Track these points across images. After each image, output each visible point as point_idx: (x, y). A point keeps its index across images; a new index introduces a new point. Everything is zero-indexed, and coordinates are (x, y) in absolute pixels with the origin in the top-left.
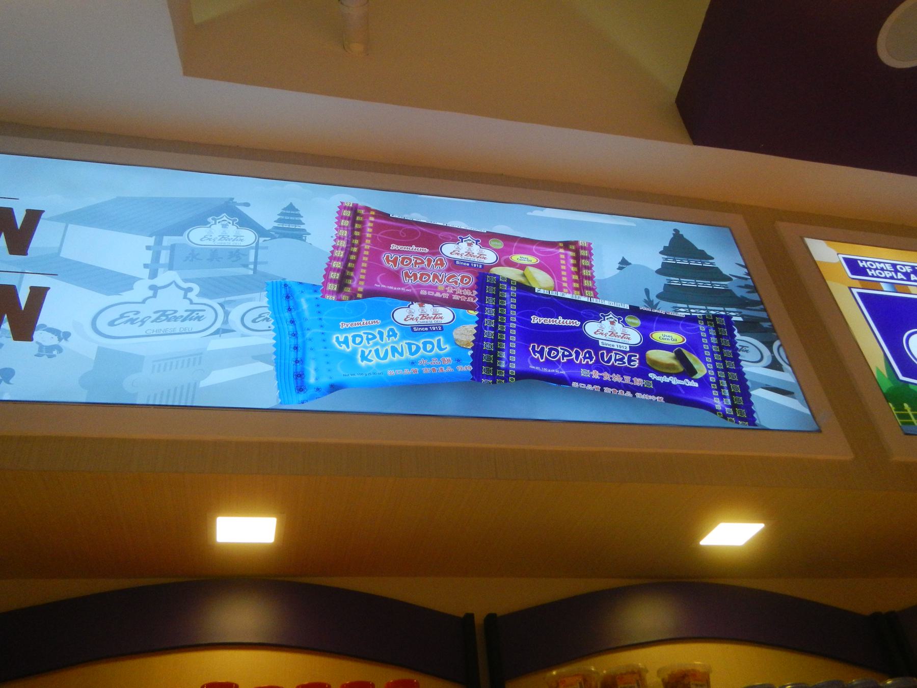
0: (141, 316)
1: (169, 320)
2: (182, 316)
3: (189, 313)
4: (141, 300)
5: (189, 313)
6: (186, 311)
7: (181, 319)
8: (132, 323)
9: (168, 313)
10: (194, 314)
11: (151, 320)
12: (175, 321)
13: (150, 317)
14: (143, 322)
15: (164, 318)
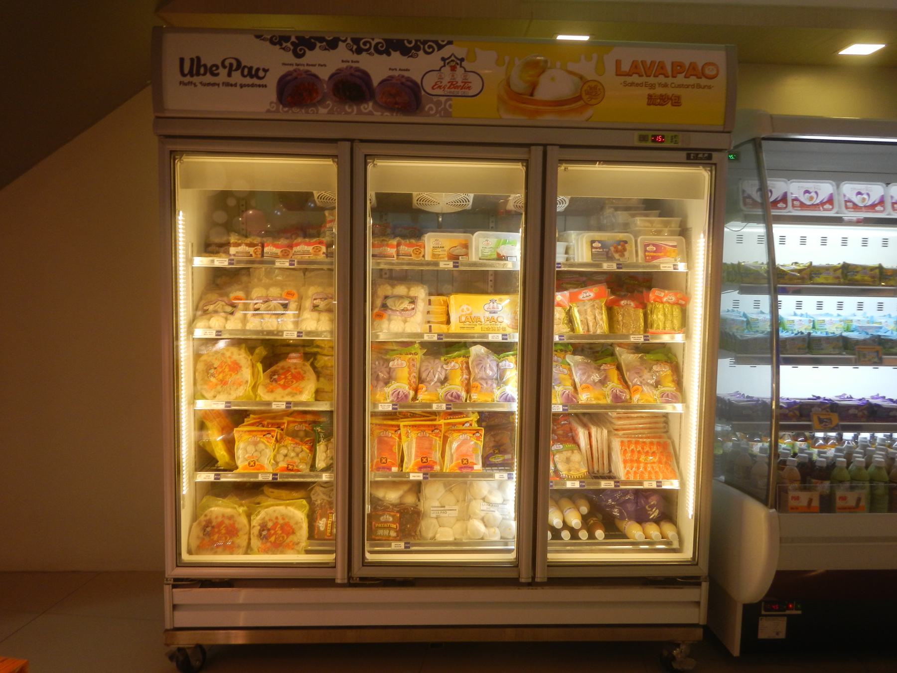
0: (443, 84)
1: (455, 88)
2: (460, 86)
3: (463, 84)
4: (438, 69)
5: (463, 84)
6: (462, 82)
7: (461, 87)
8: (440, 89)
9: (454, 83)
10: (466, 85)
11: (448, 86)
12: (458, 89)
13: (446, 85)
14: (444, 88)
15: (452, 86)
